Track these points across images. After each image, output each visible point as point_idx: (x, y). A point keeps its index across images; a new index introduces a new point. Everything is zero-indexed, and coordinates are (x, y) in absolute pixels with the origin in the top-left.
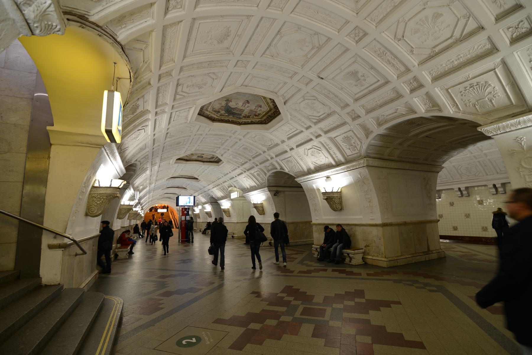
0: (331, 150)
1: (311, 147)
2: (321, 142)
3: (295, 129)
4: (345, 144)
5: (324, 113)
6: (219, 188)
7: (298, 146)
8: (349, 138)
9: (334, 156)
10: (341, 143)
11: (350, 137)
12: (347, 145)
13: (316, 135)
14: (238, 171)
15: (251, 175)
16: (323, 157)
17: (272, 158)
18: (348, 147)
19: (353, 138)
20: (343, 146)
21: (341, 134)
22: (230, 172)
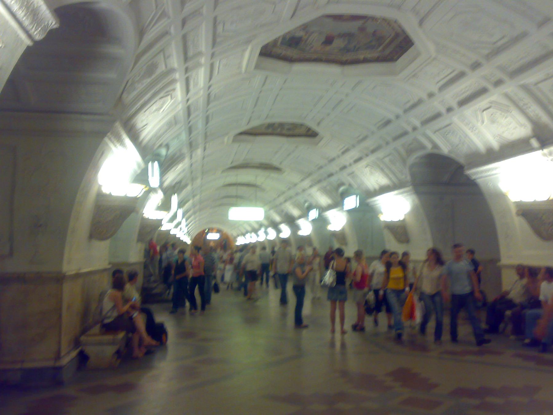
3: (450, 71)
5: (503, 37)
7: (463, 103)
14: (354, 154)
17: (415, 129)
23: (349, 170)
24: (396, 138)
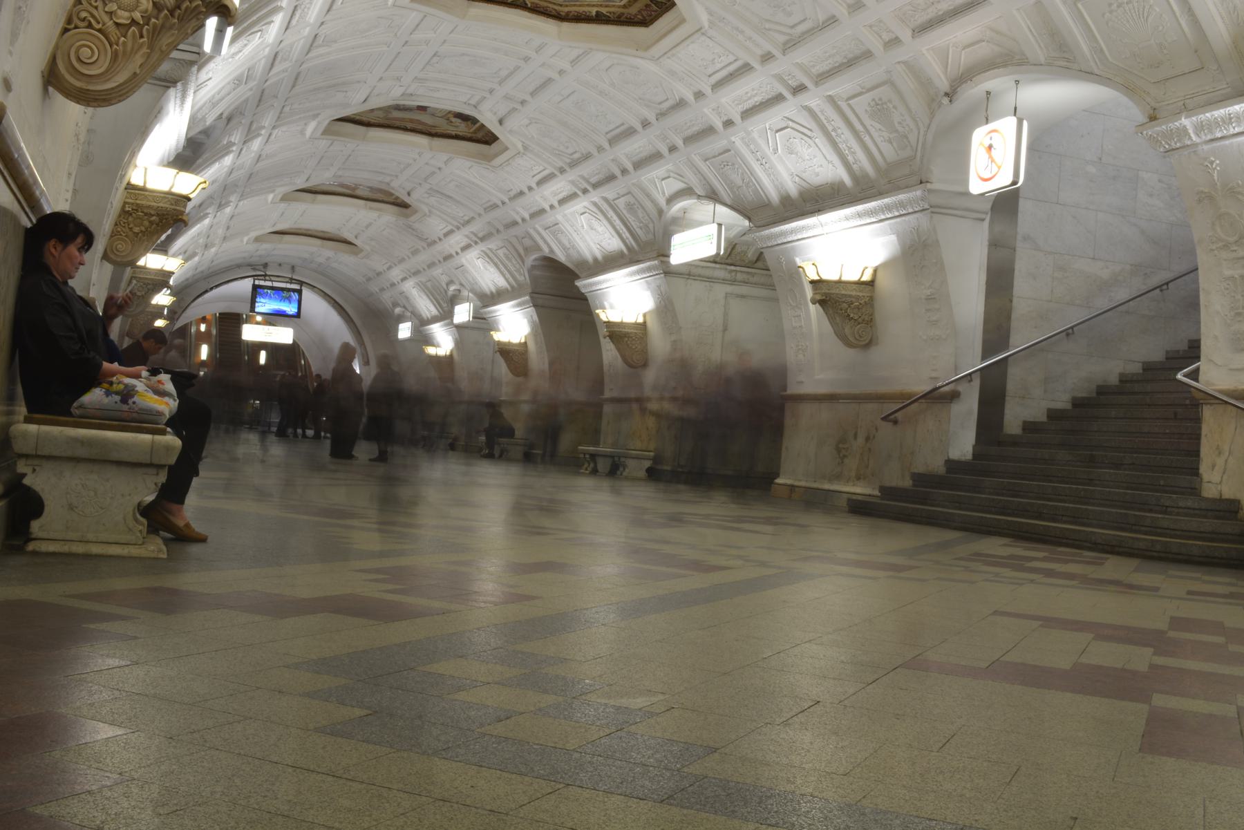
0: (840, 137)
2: (809, 110)
3: (731, 58)
4: (878, 126)
6: (488, 252)
7: (747, 114)
9: (850, 158)
11: (888, 104)
13: (793, 83)
14: (560, 186)
15: (605, 206)
18: (886, 134)
19: (895, 107)
21: (864, 90)
22: (530, 189)
23: (549, 219)
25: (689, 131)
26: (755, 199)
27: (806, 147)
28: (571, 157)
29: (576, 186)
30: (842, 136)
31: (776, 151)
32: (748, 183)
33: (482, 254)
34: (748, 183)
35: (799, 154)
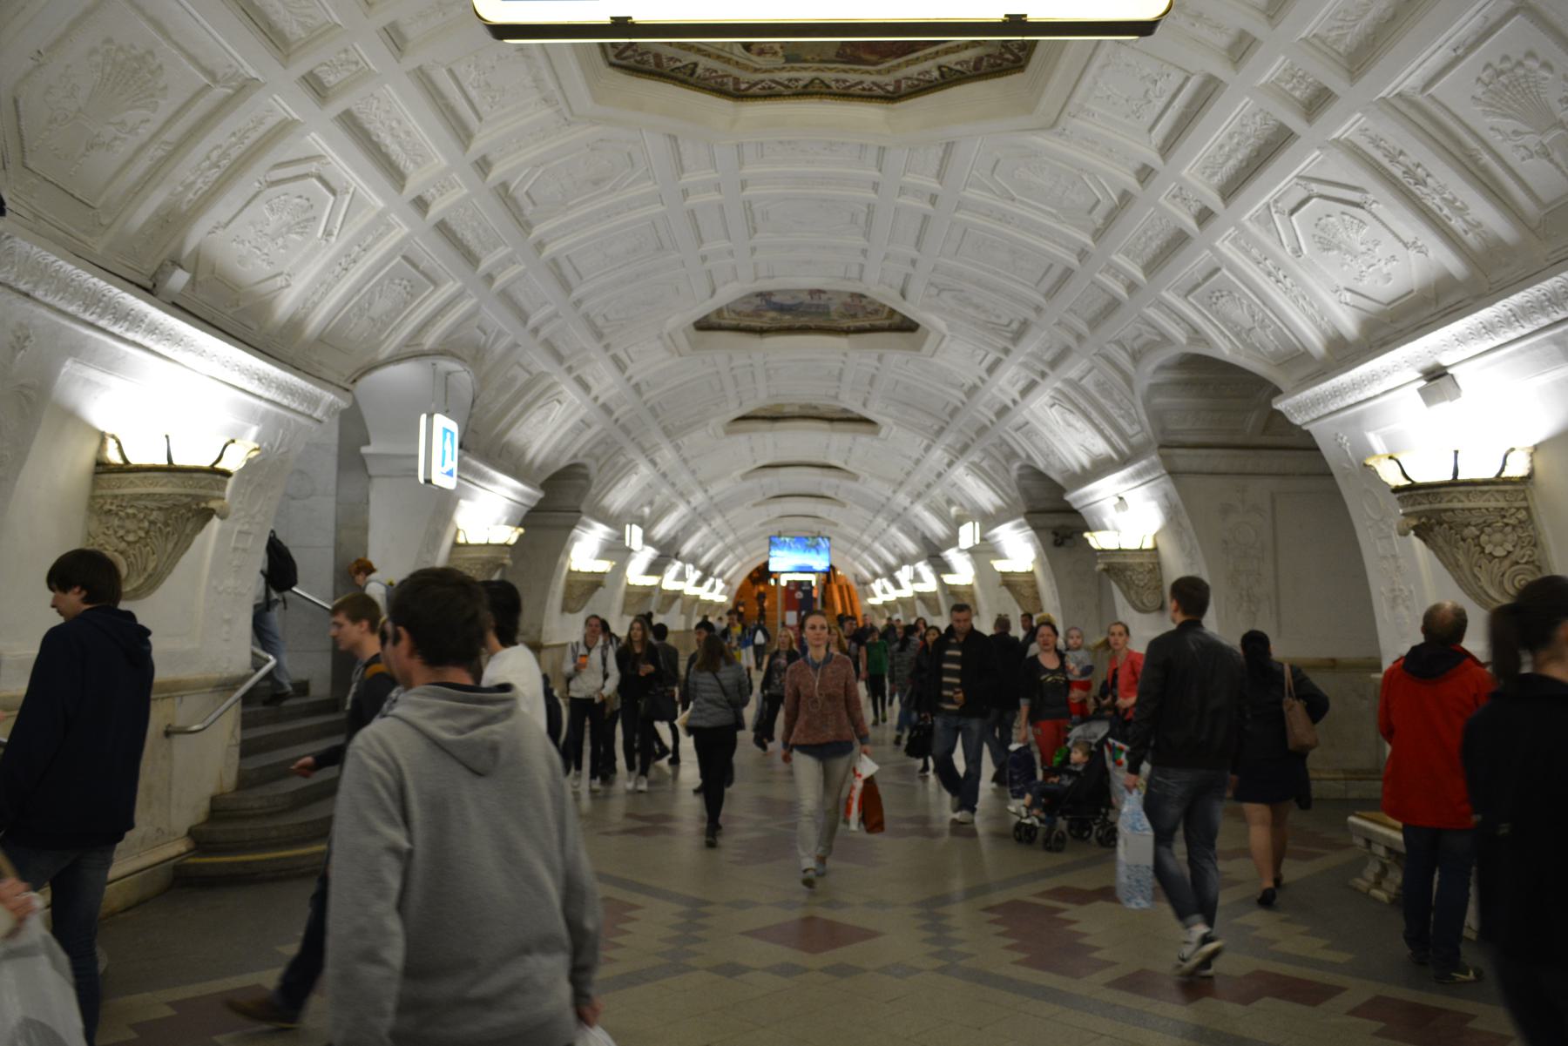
1: (1301, 194)
7: (1231, 189)
8: (1520, 72)
9: (1457, 224)
10: (1484, 122)
12: (1523, 128)
16: (1388, 245)
20: (1495, 139)
23: (1018, 418)
24: (1095, 323)
25: (1148, 250)
26: (1280, 347)
27: (1355, 227)
28: (1009, 329)
29: (1032, 369)
30: (1429, 180)
31: (1297, 251)
32: (1263, 321)
33: (1058, 396)
34: (1263, 321)
35: (1343, 246)
